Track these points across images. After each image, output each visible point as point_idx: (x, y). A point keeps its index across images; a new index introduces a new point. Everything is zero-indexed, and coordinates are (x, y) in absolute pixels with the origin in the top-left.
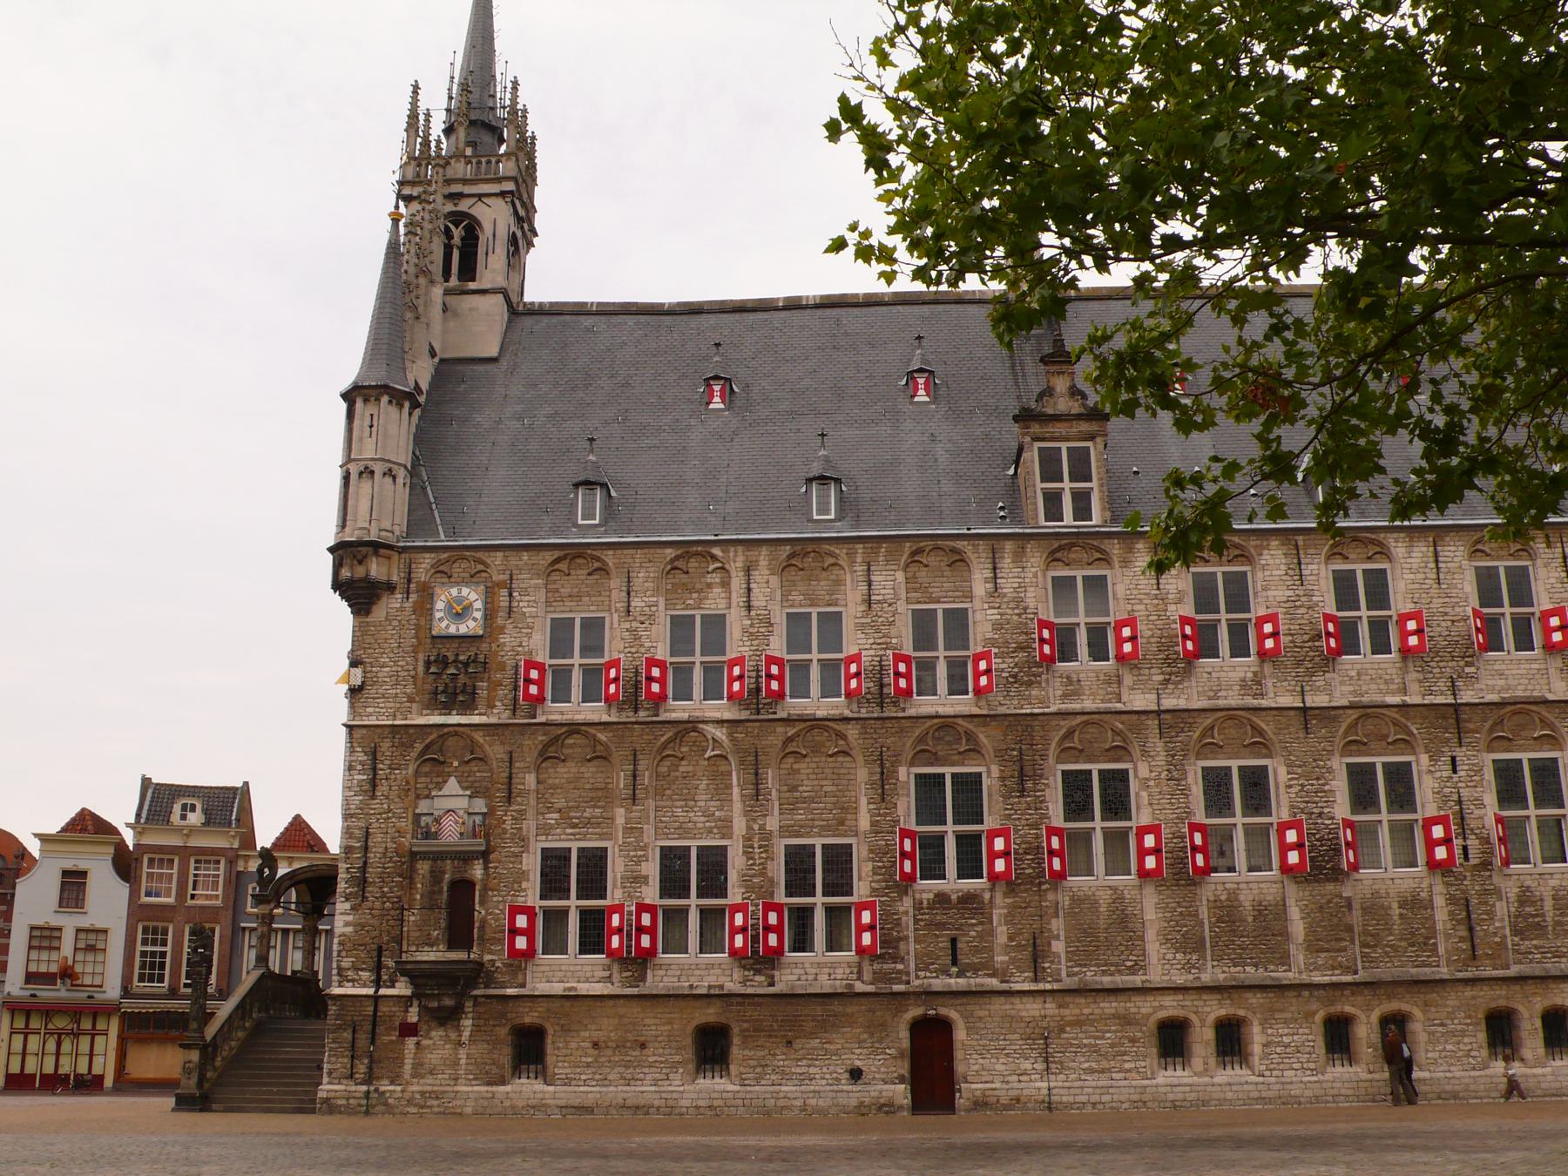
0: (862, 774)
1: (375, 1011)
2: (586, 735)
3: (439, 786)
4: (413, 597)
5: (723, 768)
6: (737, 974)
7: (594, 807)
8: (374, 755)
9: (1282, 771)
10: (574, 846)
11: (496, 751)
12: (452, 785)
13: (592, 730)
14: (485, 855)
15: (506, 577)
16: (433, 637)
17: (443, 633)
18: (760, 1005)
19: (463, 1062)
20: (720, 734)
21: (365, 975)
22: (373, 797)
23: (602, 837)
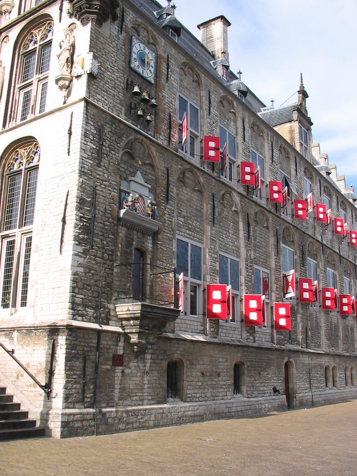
0: (272, 240)
1: (98, 343)
2: (194, 175)
3: (134, 174)
4: (124, 34)
5: (236, 218)
6: (245, 335)
7: (197, 221)
8: (100, 130)
9: (338, 275)
10: (190, 242)
11: (160, 164)
12: (139, 177)
13: (198, 173)
14: (155, 235)
15: (165, 56)
16: (131, 68)
17: (136, 69)
18: (252, 352)
19: (146, 386)
20: (237, 199)
21: (91, 312)
22: (99, 165)
23: (201, 241)
